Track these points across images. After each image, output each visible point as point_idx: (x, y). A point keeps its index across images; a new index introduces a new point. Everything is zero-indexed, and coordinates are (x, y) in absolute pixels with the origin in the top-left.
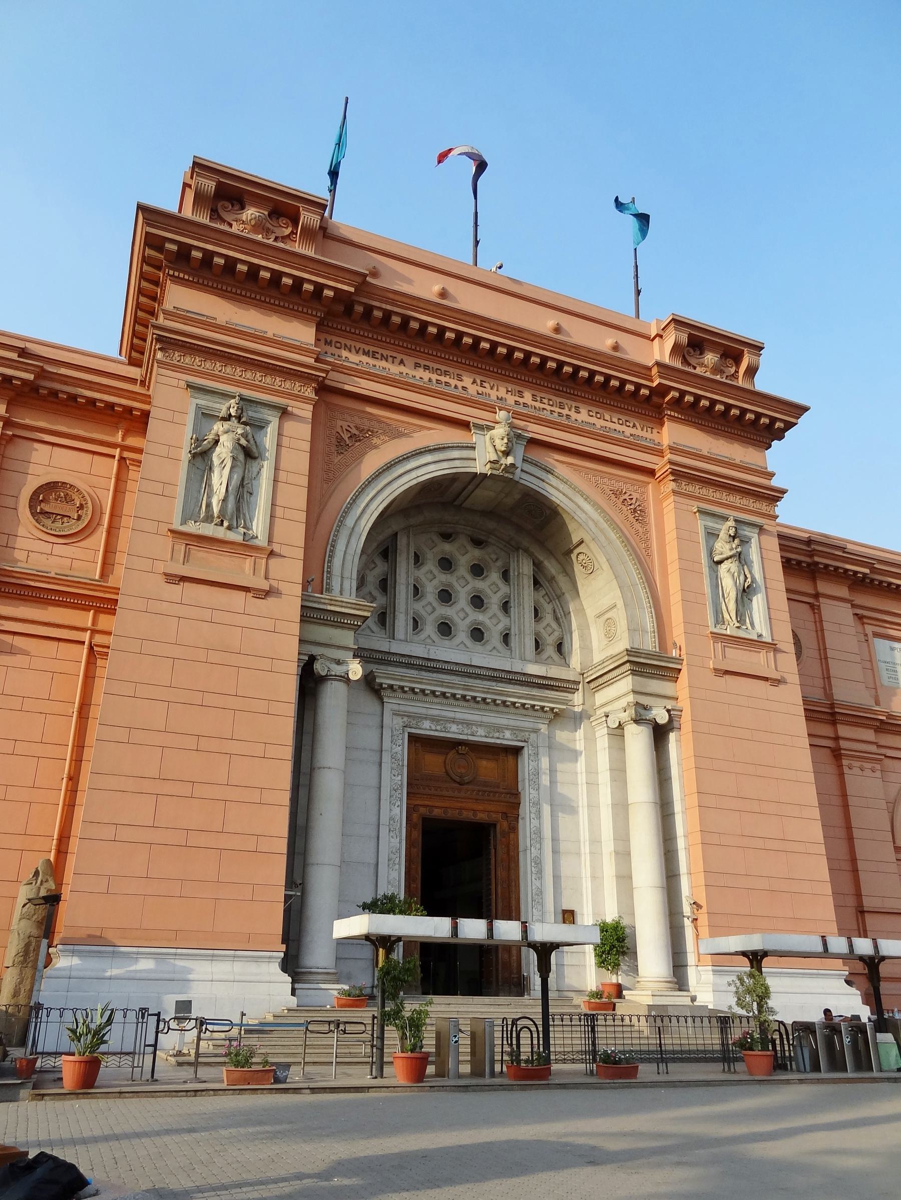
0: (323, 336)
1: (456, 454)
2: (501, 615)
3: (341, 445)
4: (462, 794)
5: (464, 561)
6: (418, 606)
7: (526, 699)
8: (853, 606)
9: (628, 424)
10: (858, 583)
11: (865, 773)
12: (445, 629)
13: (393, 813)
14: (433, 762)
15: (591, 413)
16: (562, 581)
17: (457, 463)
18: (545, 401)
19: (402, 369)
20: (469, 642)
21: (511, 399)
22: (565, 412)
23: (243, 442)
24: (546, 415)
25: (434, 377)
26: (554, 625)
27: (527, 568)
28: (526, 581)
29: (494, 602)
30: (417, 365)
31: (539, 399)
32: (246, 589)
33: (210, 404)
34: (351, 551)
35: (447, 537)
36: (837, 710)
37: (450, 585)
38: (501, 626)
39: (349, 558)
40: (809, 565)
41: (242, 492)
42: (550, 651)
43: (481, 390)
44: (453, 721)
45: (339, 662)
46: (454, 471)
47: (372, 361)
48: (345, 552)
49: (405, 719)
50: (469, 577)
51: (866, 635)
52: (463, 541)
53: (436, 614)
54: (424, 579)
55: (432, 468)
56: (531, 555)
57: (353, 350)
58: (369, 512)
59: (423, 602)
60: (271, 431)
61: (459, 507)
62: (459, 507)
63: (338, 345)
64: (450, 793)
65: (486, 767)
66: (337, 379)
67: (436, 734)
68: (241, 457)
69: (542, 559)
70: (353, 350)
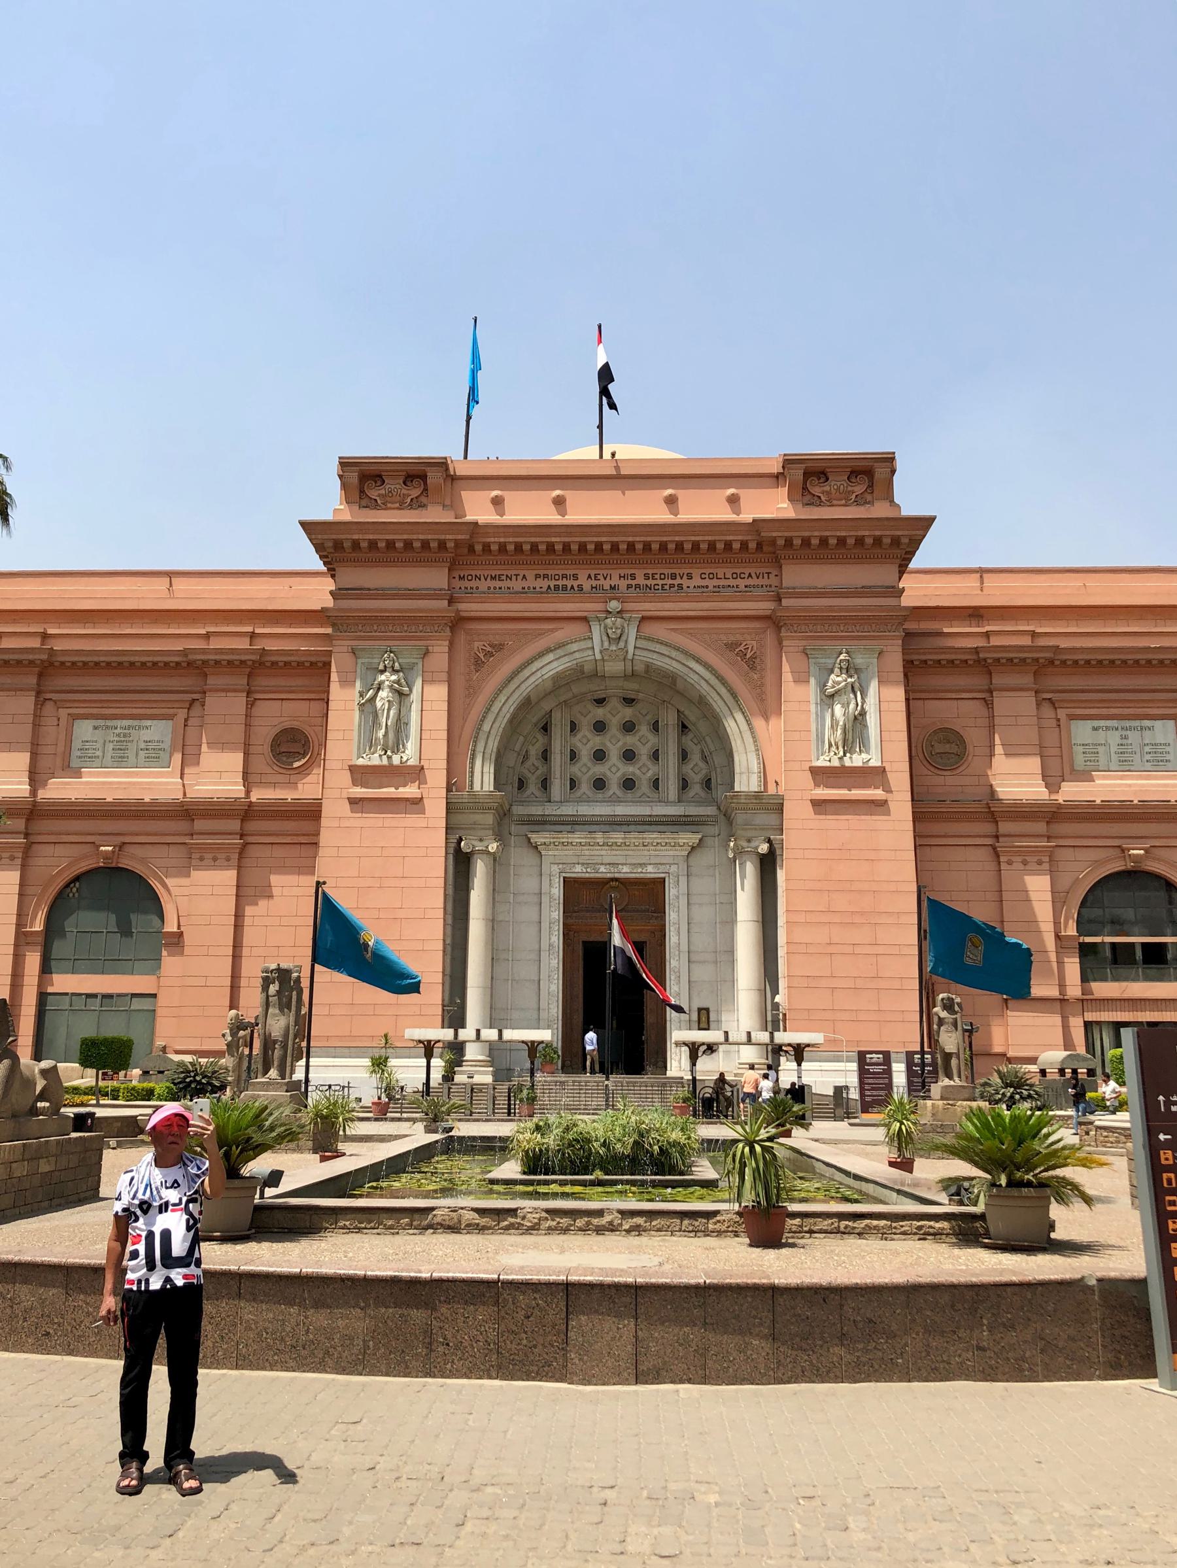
0: (456, 574)
1: (575, 647)
2: (649, 764)
3: (478, 664)
5: (614, 722)
6: (575, 769)
11: (1027, 867)
12: (600, 784)
16: (703, 727)
17: (577, 655)
20: (619, 793)
21: (623, 584)
22: (676, 582)
25: (552, 583)
26: (702, 765)
27: (670, 719)
28: (670, 730)
29: (643, 752)
30: (537, 576)
34: (488, 751)
35: (600, 702)
37: (604, 745)
38: (650, 774)
41: (401, 725)
42: (696, 789)
43: (594, 583)
45: (481, 840)
47: (498, 584)
50: (619, 735)
51: (1058, 720)
52: (614, 703)
53: (591, 773)
54: (579, 744)
55: (555, 664)
58: (502, 714)
59: (578, 765)
66: (468, 608)
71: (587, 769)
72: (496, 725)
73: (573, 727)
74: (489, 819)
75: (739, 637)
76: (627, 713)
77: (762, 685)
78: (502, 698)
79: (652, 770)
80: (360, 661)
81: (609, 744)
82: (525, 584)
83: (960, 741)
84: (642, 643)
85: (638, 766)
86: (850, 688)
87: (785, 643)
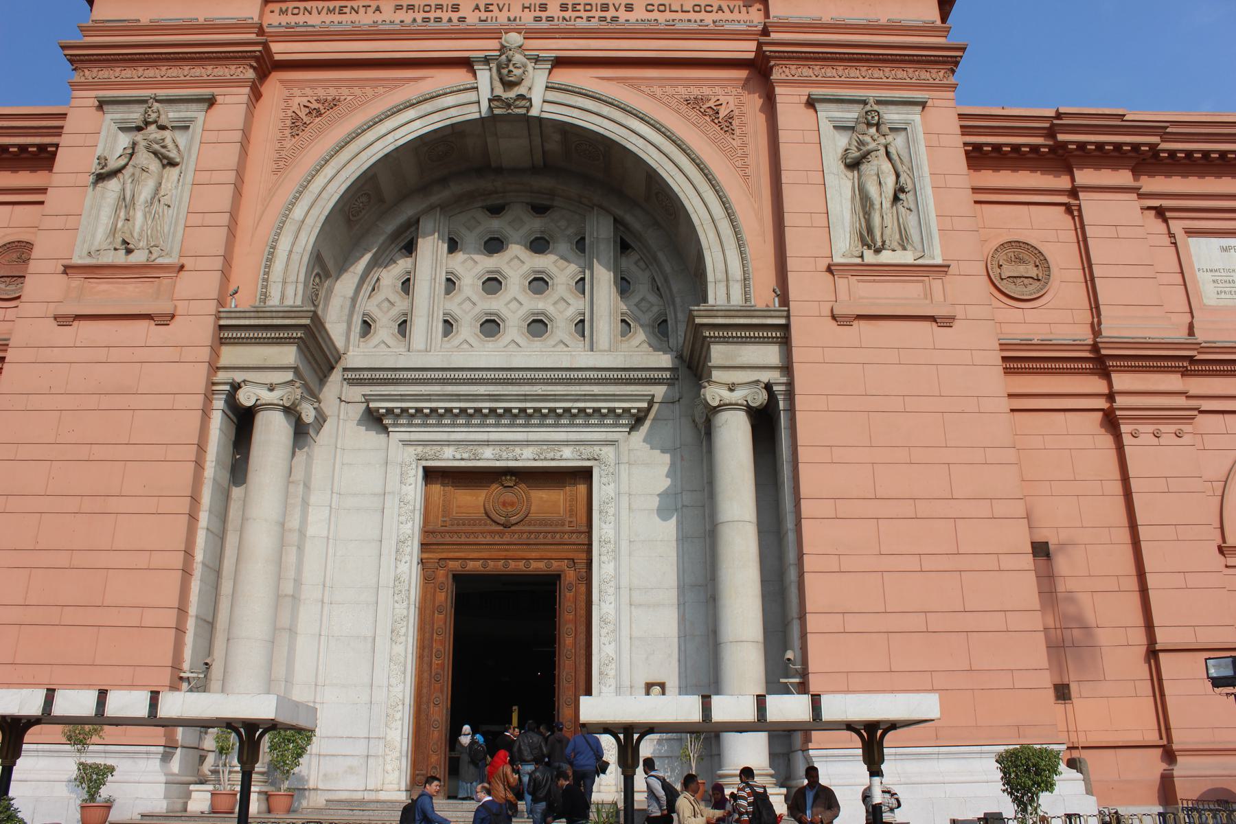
0: (276, 7)
3: (296, 125)
4: (507, 539)
6: (453, 305)
7: (585, 401)
8: (1142, 196)
9: (709, 9)
10: (1145, 160)
11: (1162, 441)
13: (399, 571)
14: (471, 500)
15: (650, 8)
17: (453, 112)
18: (580, 8)
19: (378, 17)
22: (609, 15)
23: (157, 147)
24: (581, 24)
26: (653, 298)
27: (601, 230)
28: (602, 247)
31: (570, 7)
32: (148, 317)
33: (126, 116)
34: (298, 249)
35: (496, 211)
36: (1103, 352)
38: (571, 312)
39: (295, 257)
40: (1052, 149)
43: (484, 15)
44: (488, 443)
46: (448, 122)
47: (337, 18)
48: (291, 252)
49: (420, 449)
51: (1171, 235)
55: (417, 124)
56: (608, 211)
57: (314, 11)
58: (324, 195)
60: (197, 127)
61: (499, 171)
62: (499, 171)
63: (296, 11)
64: (489, 539)
65: (545, 500)
67: (463, 464)
68: (154, 165)
69: (619, 212)
70: (314, 11)
71: (471, 303)
72: (315, 212)
73: (453, 246)
74: (288, 355)
75: (706, 91)
76: (536, 225)
77: (745, 155)
78: (329, 171)
79: (577, 305)
80: (108, 117)
81: (506, 270)
82: (378, 17)
83: (1042, 261)
84: (552, 96)
85: (551, 300)
86: (883, 150)
87: (778, 90)
